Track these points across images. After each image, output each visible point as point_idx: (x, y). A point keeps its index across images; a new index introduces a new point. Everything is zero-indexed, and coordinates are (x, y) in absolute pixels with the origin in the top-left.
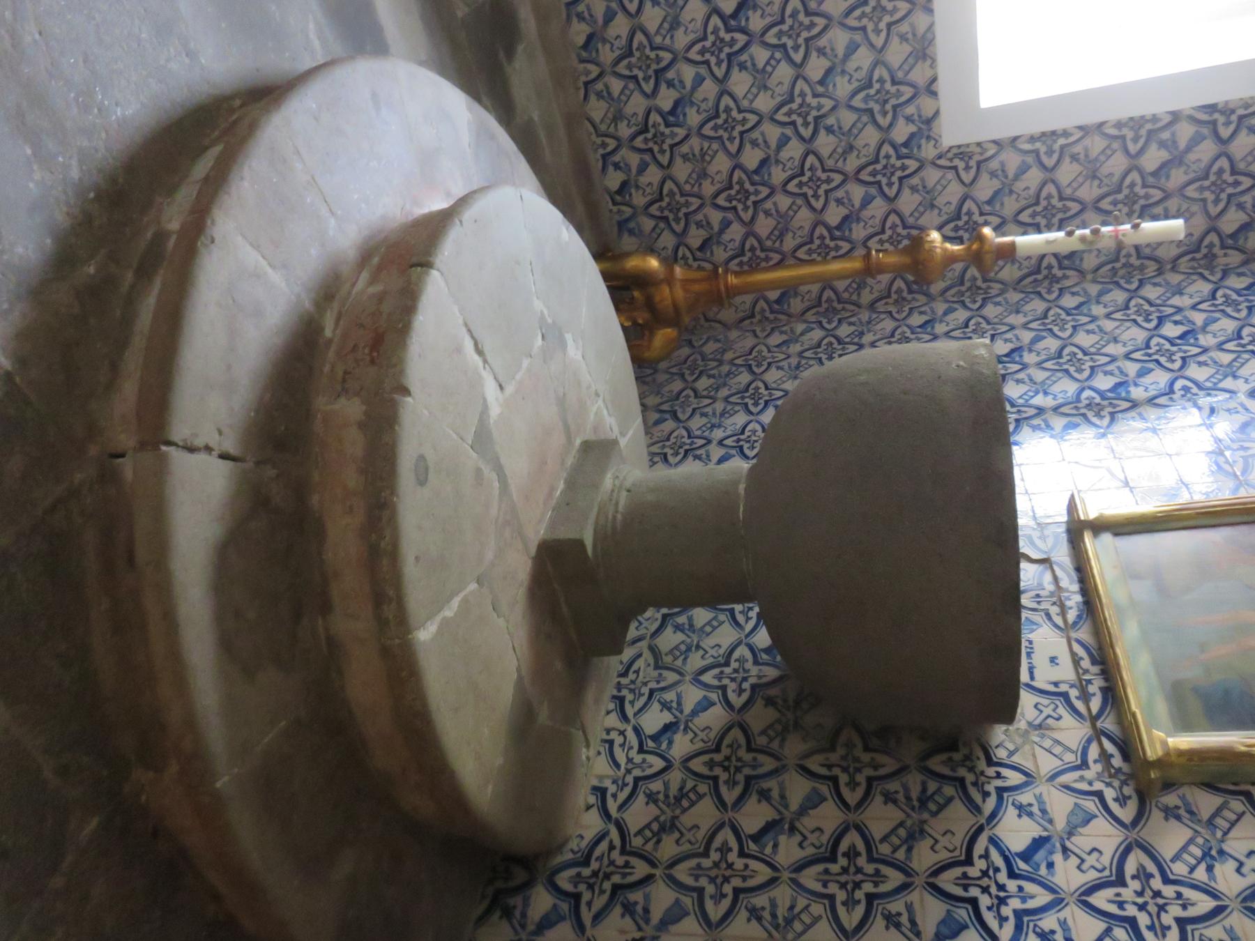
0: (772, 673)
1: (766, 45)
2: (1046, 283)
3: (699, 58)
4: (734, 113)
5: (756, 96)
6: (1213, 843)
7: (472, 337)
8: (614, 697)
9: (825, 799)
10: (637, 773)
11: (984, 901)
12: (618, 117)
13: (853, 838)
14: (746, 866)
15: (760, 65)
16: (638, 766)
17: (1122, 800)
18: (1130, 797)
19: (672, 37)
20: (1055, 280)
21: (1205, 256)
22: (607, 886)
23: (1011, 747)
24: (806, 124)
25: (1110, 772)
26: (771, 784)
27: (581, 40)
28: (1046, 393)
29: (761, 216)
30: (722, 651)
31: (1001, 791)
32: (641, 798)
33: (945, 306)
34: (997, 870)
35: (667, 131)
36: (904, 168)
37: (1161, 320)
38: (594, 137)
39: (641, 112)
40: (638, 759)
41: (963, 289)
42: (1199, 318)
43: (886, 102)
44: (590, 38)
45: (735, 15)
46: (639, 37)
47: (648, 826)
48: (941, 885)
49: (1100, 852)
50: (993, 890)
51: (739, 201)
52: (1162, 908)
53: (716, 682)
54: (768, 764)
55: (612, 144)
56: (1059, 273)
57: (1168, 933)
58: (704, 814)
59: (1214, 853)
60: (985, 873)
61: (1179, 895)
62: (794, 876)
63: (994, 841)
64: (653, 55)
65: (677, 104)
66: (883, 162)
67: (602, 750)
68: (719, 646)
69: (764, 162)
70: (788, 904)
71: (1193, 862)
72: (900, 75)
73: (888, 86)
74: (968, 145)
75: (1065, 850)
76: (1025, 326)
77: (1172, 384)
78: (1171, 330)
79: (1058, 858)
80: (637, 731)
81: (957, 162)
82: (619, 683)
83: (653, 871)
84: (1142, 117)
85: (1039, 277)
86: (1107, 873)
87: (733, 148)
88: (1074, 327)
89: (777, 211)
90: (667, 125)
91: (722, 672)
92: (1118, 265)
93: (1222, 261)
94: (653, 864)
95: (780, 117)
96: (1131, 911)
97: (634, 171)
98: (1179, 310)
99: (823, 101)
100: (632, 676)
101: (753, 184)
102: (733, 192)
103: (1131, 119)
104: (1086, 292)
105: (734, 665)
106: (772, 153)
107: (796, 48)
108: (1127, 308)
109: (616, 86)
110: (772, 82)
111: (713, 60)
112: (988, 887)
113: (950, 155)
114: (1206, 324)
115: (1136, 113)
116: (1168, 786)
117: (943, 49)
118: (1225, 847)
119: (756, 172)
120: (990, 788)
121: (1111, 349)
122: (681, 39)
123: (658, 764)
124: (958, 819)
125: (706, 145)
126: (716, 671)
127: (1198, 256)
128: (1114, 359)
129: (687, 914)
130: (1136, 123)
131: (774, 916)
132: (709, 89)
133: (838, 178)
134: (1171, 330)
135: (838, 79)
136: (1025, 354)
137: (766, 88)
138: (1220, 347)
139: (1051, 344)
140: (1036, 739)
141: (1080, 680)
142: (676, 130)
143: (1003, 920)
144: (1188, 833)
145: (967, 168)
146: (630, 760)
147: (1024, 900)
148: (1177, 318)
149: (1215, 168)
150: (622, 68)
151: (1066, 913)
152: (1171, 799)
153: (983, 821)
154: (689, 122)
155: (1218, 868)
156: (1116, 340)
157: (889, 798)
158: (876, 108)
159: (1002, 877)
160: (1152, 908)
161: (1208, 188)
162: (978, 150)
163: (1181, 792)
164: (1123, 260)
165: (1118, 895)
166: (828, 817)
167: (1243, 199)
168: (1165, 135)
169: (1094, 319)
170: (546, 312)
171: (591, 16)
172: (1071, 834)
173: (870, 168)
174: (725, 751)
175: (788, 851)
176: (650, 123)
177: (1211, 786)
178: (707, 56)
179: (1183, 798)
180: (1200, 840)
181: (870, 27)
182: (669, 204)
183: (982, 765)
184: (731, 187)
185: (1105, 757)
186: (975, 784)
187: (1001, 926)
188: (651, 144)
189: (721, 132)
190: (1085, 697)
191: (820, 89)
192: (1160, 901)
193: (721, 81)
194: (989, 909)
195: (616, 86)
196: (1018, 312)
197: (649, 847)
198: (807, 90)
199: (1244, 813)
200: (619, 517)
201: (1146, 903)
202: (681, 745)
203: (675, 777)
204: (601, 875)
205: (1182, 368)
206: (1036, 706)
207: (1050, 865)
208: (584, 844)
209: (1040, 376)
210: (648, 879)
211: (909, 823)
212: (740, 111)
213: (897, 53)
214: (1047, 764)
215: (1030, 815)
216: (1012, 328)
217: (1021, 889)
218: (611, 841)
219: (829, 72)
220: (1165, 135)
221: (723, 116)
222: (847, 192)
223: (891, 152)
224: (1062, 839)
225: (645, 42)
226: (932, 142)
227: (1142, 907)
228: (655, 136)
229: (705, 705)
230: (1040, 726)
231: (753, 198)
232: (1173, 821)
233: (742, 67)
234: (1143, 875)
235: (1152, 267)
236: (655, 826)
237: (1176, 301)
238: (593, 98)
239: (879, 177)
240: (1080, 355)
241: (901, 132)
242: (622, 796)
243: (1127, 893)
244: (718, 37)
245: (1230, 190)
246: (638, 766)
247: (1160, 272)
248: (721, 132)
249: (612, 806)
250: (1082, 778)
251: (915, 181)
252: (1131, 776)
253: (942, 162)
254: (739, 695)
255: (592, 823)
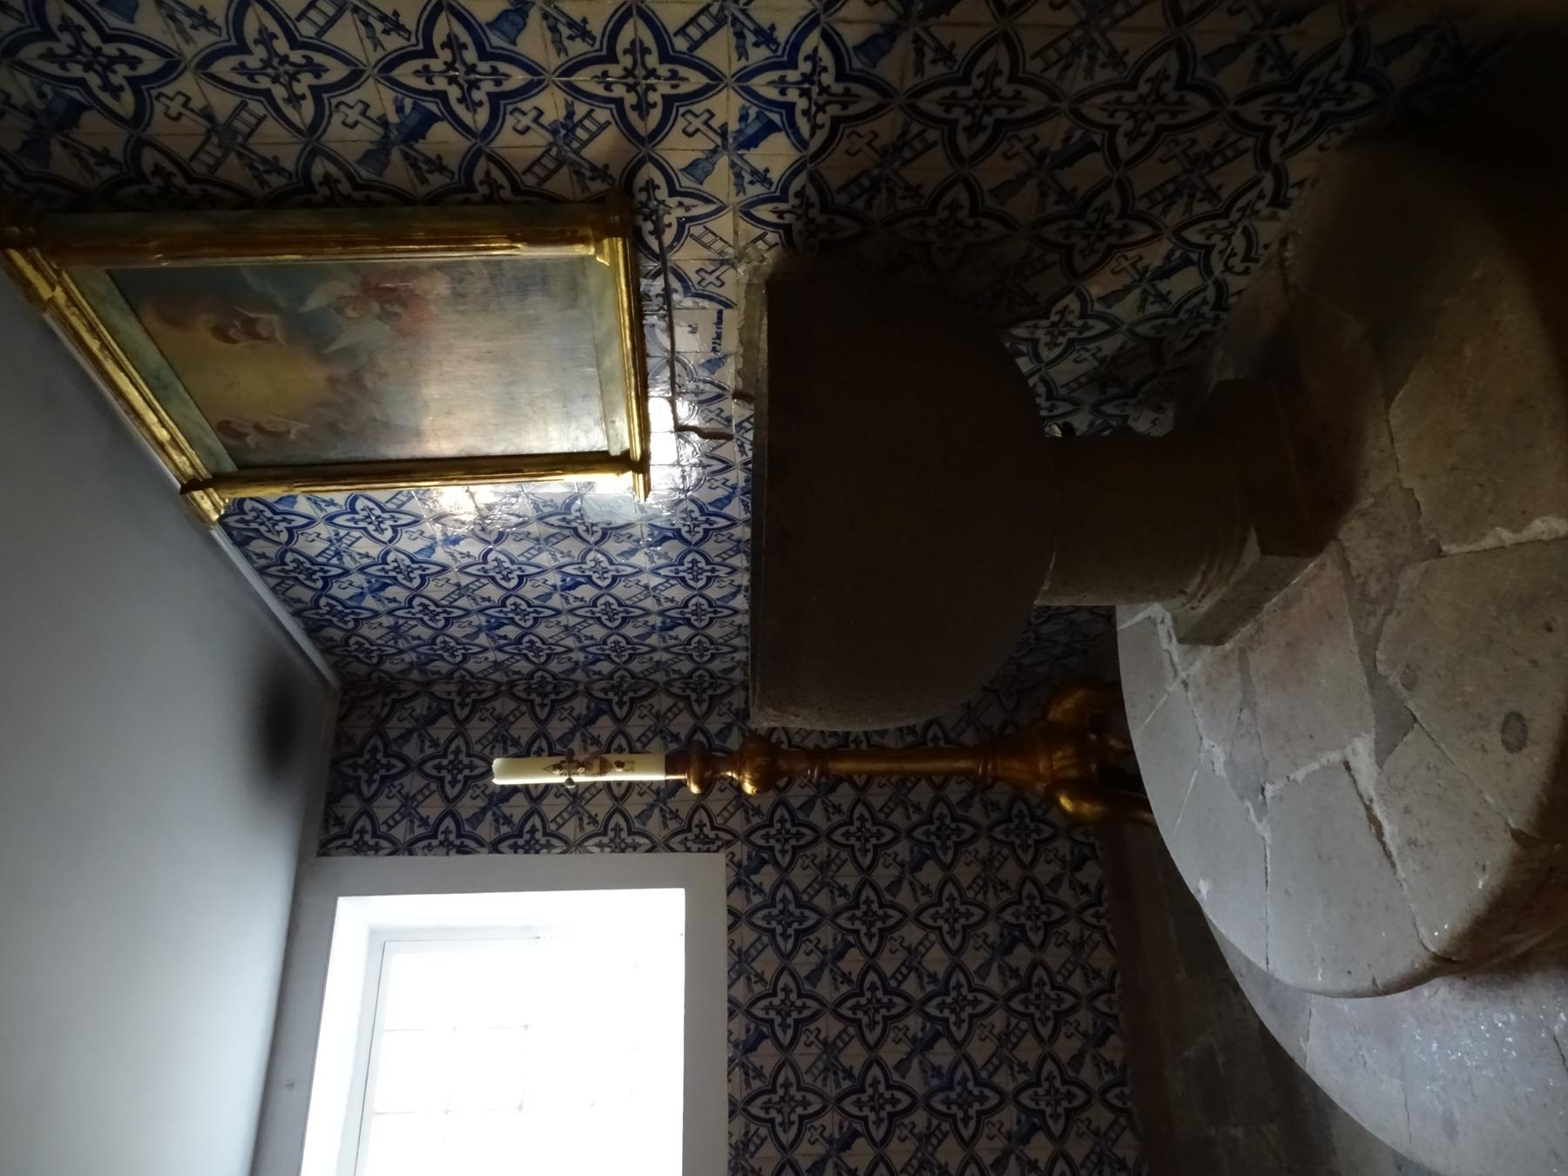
0: (1020, 332)
1: (906, 997)
2: (625, 686)
3: (980, 996)
4: (946, 928)
5: (921, 943)
6: (561, 143)
7: (1383, 844)
8: (1226, 310)
9: (991, 191)
10: (1222, 223)
11: (827, 79)
12: (1078, 946)
13: (966, 147)
14: (1111, 115)
15: (913, 975)
16: (1219, 231)
17: (651, 186)
18: (641, 189)
19: (1008, 1025)
20: (616, 689)
21: (468, 695)
22: (1305, 89)
23: (760, 244)
24: (868, 902)
25: (654, 216)
26: (1052, 208)
27: (1114, 1040)
28: (646, 587)
29: (924, 806)
30: (1074, 355)
31: (783, 198)
32: (1225, 194)
33: (731, 676)
34: (805, 113)
35: (1023, 920)
36: (767, 837)
37: (519, 640)
38: (1109, 927)
39: (1051, 948)
40: (1216, 239)
41: (710, 692)
42: (483, 639)
43: (782, 912)
44: (1101, 1042)
45: (937, 1035)
46: (1045, 1032)
47: (1227, 161)
48: (874, 94)
49: (684, 131)
50: (815, 89)
51: (948, 827)
52: (629, 72)
53: (1091, 322)
54: (1052, 232)
55: (1088, 916)
56: (611, 695)
57: (628, 46)
58: (1144, 179)
59: (563, 132)
60: (821, 108)
61: (608, 87)
62: (1055, 105)
63: (801, 143)
64: (1032, 1009)
65: (1009, 950)
66: (788, 847)
67: (1261, 251)
68: (1075, 361)
69: (917, 867)
70: (1070, 72)
71: (587, 123)
72: (765, 939)
73: (779, 929)
74: (699, 850)
75: (723, 132)
76: (653, 649)
77: (520, 583)
78: (511, 631)
79: (734, 126)
80: (1207, 270)
81: (712, 835)
82: (1215, 325)
83: (1236, 108)
84: (526, 852)
85: (631, 694)
86: (682, 110)
87: (950, 889)
88: (605, 643)
89: (906, 809)
90: (1022, 927)
91: (1081, 333)
92: (552, 696)
93: (453, 688)
94: (1235, 117)
95: (897, 916)
96: (664, 70)
97: (1066, 883)
98: (500, 649)
99: (847, 925)
100: (1196, 332)
101: (931, 845)
102: (954, 838)
103: (537, 852)
104: (588, 675)
105: (1062, 340)
106: (908, 876)
107: (873, 987)
108: (549, 656)
109: (1076, 982)
110: (902, 955)
111: (964, 991)
112: (819, 94)
113: (719, 843)
114: (476, 634)
115: (532, 857)
116: (599, 200)
117: (721, 961)
118: (550, 138)
119: (927, 858)
120: (793, 201)
121: (573, 621)
122: (998, 1020)
123: (1193, 235)
124: (836, 169)
125: (980, 897)
126: (1086, 334)
127: (474, 696)
128: (571, 611)
129: (1205, 57)
130: (530, 848)
131: (1093, 58)
132: (972, 960)
133: (837, 836)
134: (511, 631)
135: (831, 946)
136: (659, 624)
137: (908, 949)
138: (467, 612)
139: (630, 631)
140: (730, 250)
141: (669, 310)
142: (1013, 920)
143: (813, 57)
144: (586, 153)
145: (701, 826)
146: (1228, 238)
147: (782, 79)
148: (502, 642)
149: (459, 787)
150: (1069, 1000)
151: (737, 65)
152: (597, 186)
153: (809, 166)
154: (997, 927)
155: (562, 113)
156: (566, 627)
157: (913, 191)
158: (792, 907)
159: (802, 104)
160: (640, 72)
161: (466, 767)
162: (689, 844)
163: (587, 194)
164: (547, 701)
165: (674, 87)
166: (991, 172)
167: (432, 751)
168: (505, 829)
169: (583, 649)
170: (1253, 817)
171: (1098, 1066)
172: (714, 151)
173: (802, 842)
174: (1101, 246)
175: (1052, 135)
176: (1041, 933)
177: (554, 200)
178: (970, 997)
179: (585, 188)
180: (575, 145)
181: (793, 996)
182: (1028, 836)
183: (798, 226)
184: (957, 844)
185: (658, 232)
186: (811, 205)
187: (816, 50)
188: (1043, 908)
189: (962, 909)
190: (667, 293)
191: (851, 939)
192: (630, 80)
193: (957, 966)
194: (825, 69)
195: (1076, 982)
196: (658, 663)
197: (1233, 137)
198: (865, 940)
199: (524, 173)
200: (1203, 567)
201: (646, 78)
202: (1155, 256)
203: (1174, 216)
204: (1309, 103)
205: (507, 598)
206: (723, 284)
207: (743, 118)
208: (1322, 139)
209: (649, 603)
210: (1244, 99)
211: (897, 164)
212: (939, 929)
213: (767, 963)
214: (724, 225)
215: (754, 172)
216: (667, 649)
217: (783, 92)
218: (1282, 144)
219: (840, 956)
220: (505, 829)
221: (958, 927)
222: (829, 819)
223: (779, 857)
224: (725, 147)
225: (1039, 1025)
226: (736, 860)
227: (652, 73)
228: (1038, 917)
229: (1111, 298)
230: (723, 262)
231: (933, 828)
232: (600, 165)
233: (933, 978)
234: (643, 108)
235: (519, 690)
236: (1218, 161)
237: (501, 657)
238: (1105, 973)
239: (794, 830)
240: (604, 618)
241: (767, 877)
242: (1252, 195)
243: (664, 88)
244: (958, 1016)
245: (445, 762)
246: (1219, 231)
247: (512, 684)
248: (962, 909)
249: (1268, 184)
250: (688, 209)
251: (756, 820)
252: (636, 212)
253: (727, 837)
254: (1066, 307)
255: (1300, 167)
